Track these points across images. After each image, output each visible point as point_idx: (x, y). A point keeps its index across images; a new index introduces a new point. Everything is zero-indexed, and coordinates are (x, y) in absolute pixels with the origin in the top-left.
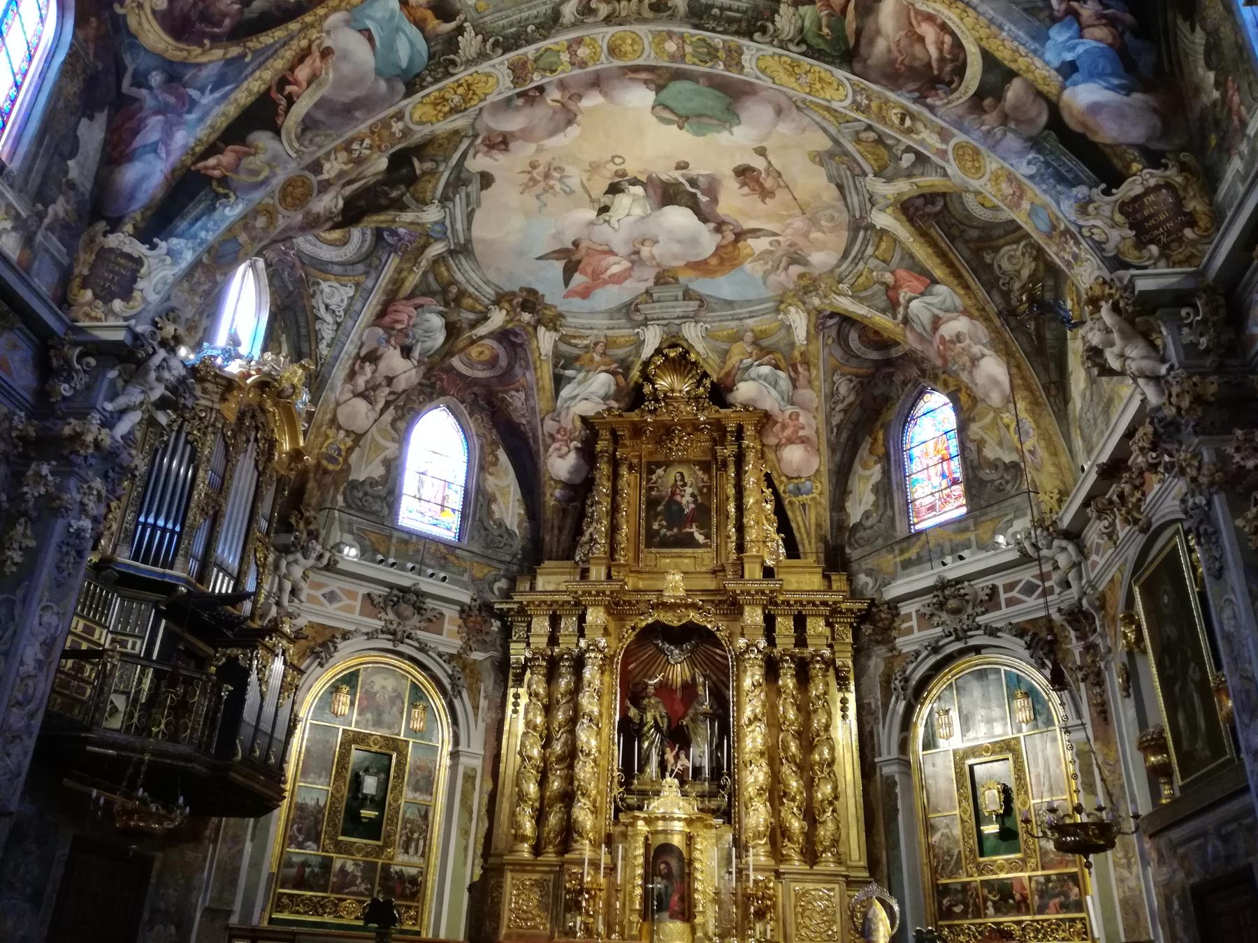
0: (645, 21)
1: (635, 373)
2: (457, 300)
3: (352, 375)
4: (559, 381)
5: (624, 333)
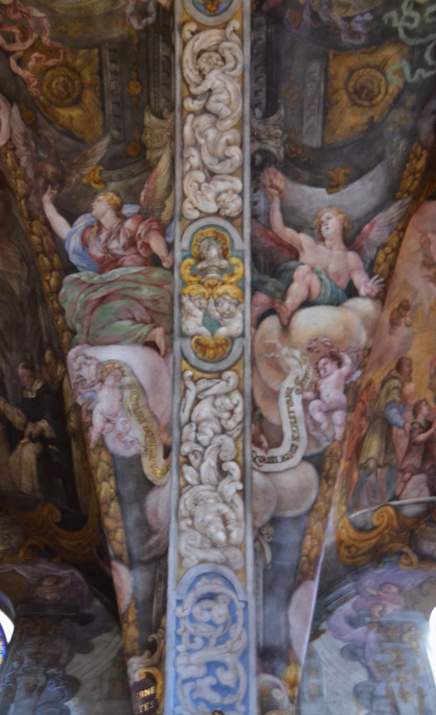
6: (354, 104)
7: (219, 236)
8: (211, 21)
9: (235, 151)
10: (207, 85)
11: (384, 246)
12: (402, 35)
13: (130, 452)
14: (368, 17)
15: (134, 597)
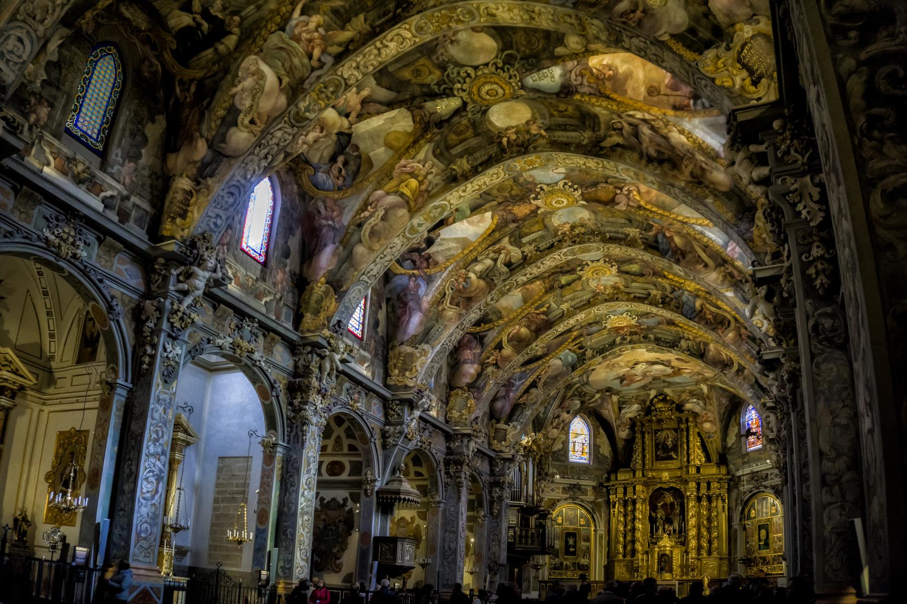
0: (642, 342)
1: (648, 403)
2: (584, 395)
3: (552, 423)
4: (620, 409)
5: (643, 393)
6: (413, 72)
7: (337, 87)
8: (414, 31)
9: (371, 68)
10: (389, 44)
11: (369, 114)
12: (446, 73)
13: (240, 107)
14: (446, 59)
15: (203, 159)
